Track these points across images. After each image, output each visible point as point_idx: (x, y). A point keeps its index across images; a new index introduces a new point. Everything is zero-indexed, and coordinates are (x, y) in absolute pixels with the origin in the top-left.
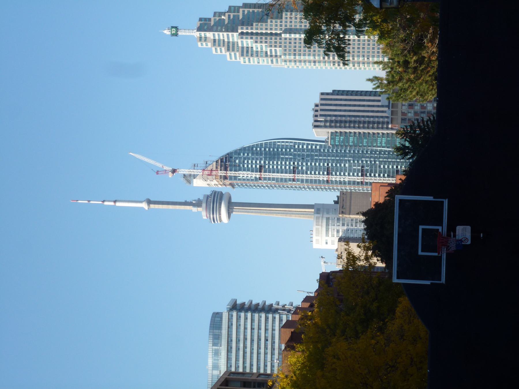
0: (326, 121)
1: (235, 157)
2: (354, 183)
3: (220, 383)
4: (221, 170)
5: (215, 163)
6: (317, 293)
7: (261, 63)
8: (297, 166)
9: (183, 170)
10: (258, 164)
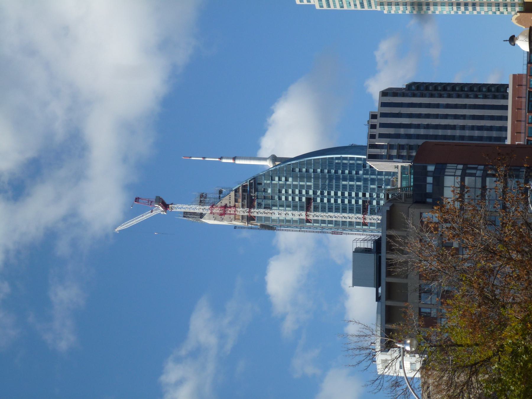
0: (390, 147)
1: (265, 184)
4: (243, 206)
5: (232, 194)
7: (346, 8)
8: (369, 199)
9: (180, 206)
10: (304, 196)
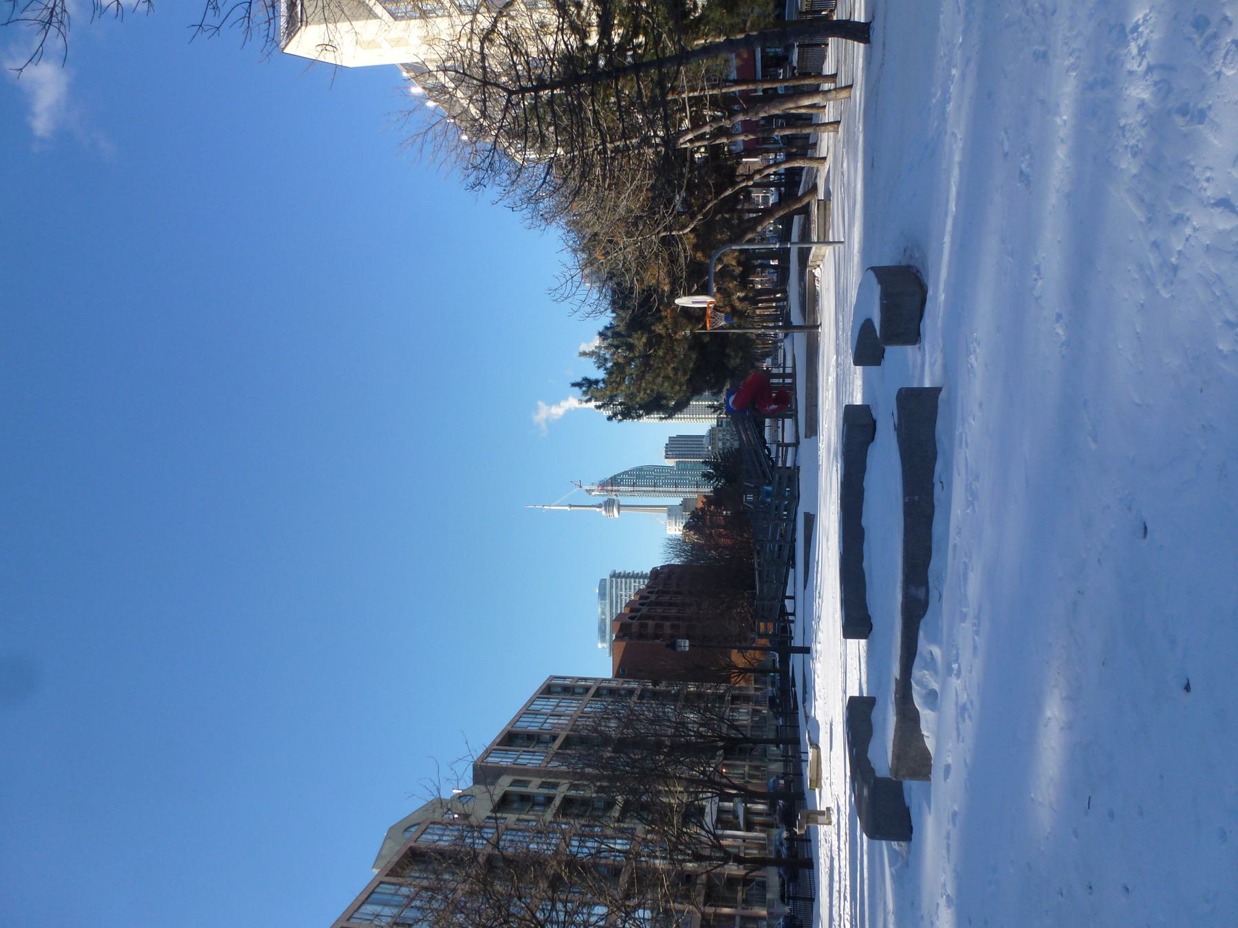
0: (673, 454)
2: (692, 492)
3: (540, 691)
6: (629, 609)
